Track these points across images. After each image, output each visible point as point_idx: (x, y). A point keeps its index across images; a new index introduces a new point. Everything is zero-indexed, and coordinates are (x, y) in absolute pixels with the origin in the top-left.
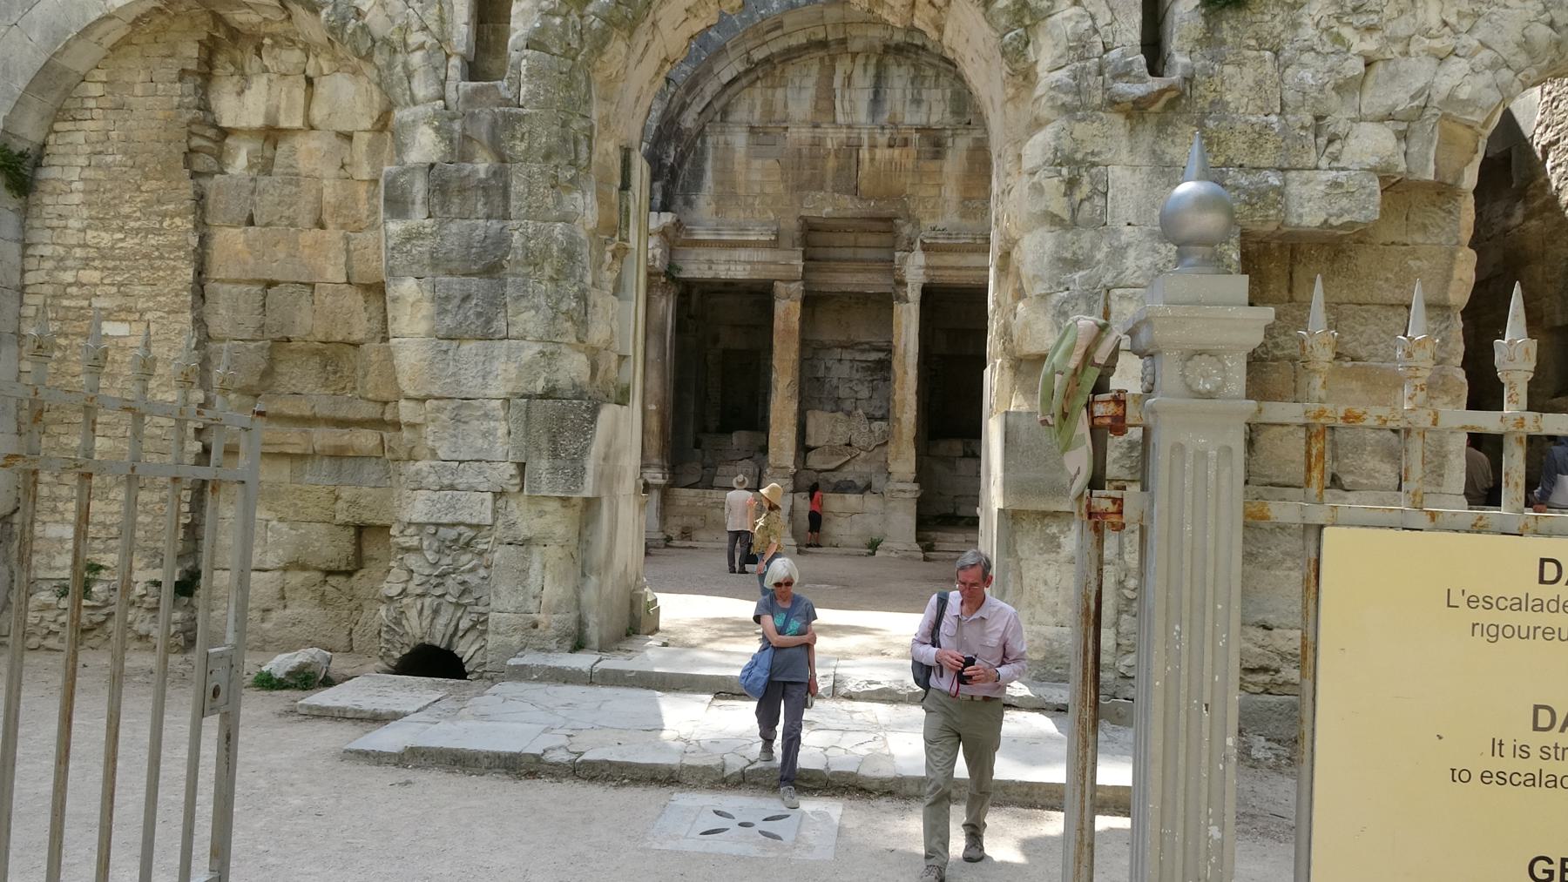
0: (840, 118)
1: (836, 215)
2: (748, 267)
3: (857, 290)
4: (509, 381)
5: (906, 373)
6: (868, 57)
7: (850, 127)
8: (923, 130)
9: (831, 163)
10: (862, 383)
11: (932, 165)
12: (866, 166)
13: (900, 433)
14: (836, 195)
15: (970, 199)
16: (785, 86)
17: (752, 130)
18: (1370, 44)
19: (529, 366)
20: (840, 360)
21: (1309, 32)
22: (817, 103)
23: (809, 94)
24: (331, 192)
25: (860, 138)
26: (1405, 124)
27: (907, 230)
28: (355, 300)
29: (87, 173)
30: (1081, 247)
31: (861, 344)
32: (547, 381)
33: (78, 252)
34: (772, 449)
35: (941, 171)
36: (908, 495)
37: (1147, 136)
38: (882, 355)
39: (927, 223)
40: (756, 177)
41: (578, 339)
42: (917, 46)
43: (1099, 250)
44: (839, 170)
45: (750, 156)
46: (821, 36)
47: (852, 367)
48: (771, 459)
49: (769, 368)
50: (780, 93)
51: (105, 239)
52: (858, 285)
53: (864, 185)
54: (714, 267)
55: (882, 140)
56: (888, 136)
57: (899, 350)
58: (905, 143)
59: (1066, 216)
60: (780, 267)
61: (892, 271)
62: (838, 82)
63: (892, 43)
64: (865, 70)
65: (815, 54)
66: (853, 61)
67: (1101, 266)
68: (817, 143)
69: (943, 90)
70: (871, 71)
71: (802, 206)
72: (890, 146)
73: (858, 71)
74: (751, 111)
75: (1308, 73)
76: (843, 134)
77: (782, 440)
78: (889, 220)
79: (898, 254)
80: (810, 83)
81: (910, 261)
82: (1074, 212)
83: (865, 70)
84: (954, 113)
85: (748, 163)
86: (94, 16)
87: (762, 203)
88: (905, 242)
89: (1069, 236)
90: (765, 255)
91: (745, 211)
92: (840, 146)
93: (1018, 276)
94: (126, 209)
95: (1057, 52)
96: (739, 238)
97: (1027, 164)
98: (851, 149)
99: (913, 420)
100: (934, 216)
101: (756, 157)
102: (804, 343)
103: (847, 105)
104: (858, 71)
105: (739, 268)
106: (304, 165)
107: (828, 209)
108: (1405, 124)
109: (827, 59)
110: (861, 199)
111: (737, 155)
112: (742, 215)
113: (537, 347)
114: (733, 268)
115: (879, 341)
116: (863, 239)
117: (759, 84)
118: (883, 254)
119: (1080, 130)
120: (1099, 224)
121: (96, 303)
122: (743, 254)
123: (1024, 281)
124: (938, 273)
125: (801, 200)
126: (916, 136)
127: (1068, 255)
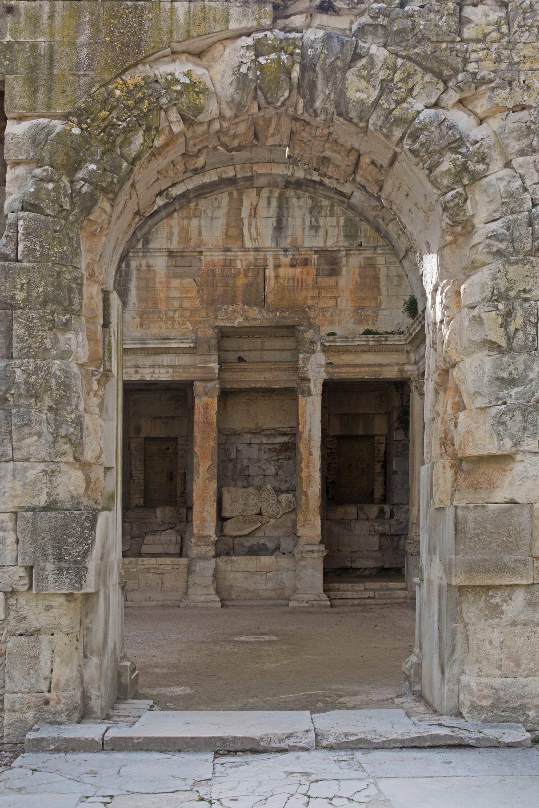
0: (248, 244)
1: (246, 324)
3: (264, 385)
4: (16, 496)
7: (257, 250)
9: (241, 281)
10: (270, 463)
12: (271, 283)
19: (34, 483)
20: (250, 444)
22: (227, 230)
23: (221, 223)
25: (265, 260)
30: (516, 369)
31: (268, 430)
32: (49, 494)
38: (286, 439)
41: (75, 458)
43: (532, 370)
44: (249, 286)
45: (172, 275)
46: (231, 174)
47: (260, 450)
49: (190, 452)
52: (265, 381)
53: (271, 298)
55: (285, 260)
56: (290, 257)
59: (503, 343)
61: (296, 369)
62: (245, 213)
63: (293, 180)
64: (269, 203)
65: (225, 189)
66: (258, 195)
67: (534, 383)
68: (228, 264)
69: (338, 218)
76: (251, 256)
78: (292, 327)
79: (301, 356)
80: (221, 213)
82: (510, 339)
83: (269, 203)
89: (505, 359)
92: (249, 265)
93: (457, 390)
95: (492, 207)
97: (466, 300)
102: (220, 431)
103: (253, 231)
104: (263, 203)
109: (235, 193)
110: (268, 310)
113: (41, 467)
115: (284, 427)
116: (269, 343)
118: (287, 356)
119: (513, 271)
123: (465, 396)
127: (505, 375)
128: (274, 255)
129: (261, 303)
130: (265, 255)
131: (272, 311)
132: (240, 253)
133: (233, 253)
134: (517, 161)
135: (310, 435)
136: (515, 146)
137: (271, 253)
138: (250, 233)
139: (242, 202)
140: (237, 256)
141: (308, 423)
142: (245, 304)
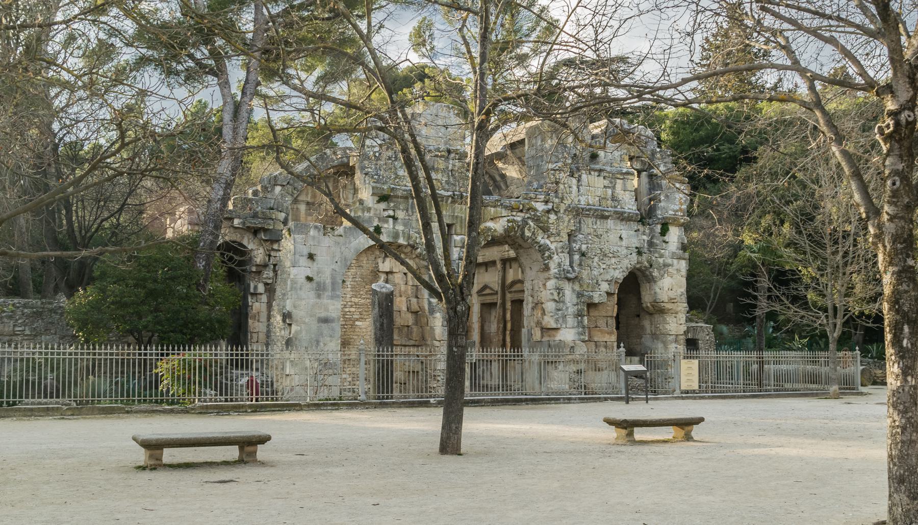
17: (308, 203)
18: (604, 266)
21: (595, 264)
24: (403, 288)
26: (609, 282)
28: (409, 315)
29: (352, 283)
33: (349, 303)
37: (571, 284)
51: (356, 300)
74: (307, 194)
75: (595, 272)
85: (306, 218)
86: (366, 247)
94: (362, 293)
106: (397, 281)
108: (609, 282)
120: (563, 302)
121: (354, 317)
134: (560, 254)
136: (560, 251)
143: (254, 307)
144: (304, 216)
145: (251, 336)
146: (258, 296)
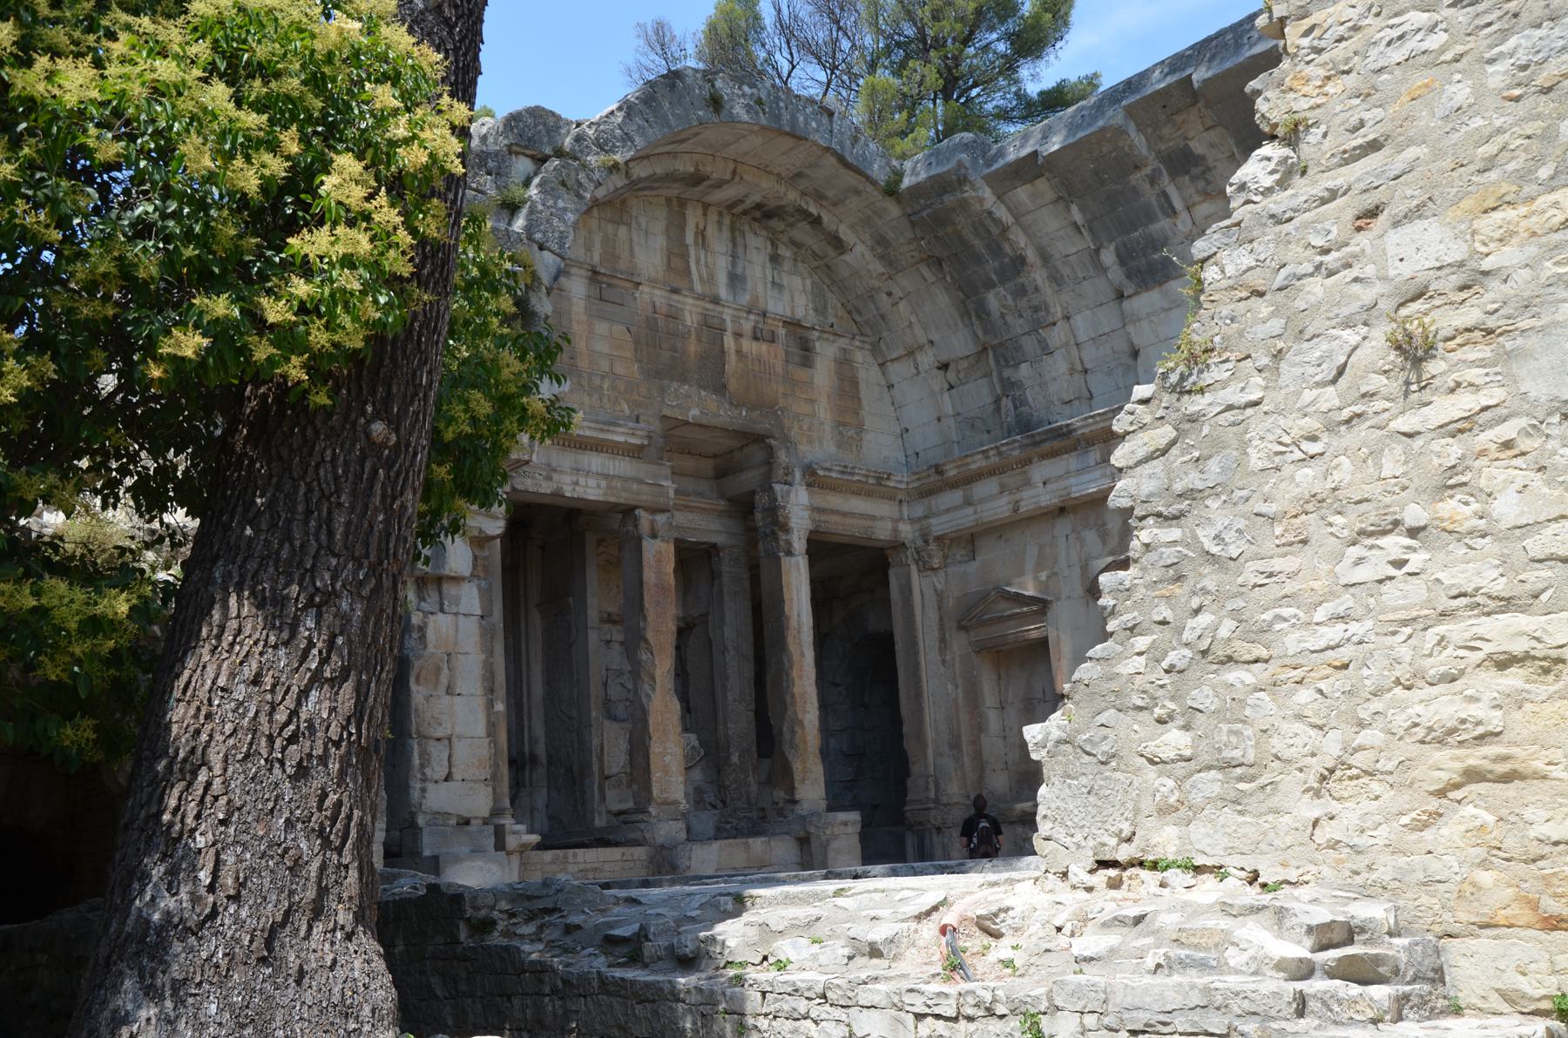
0: (698, 288)
1: (705, 422)
2: (603, 483)
5: (803, 655)
6: (720, 214)
8: (792, 324)
9: (693, 347)
11: (801, 374)
12: (732, 361)
13: (805, 742)
14: (703, 393)
15: (844, 425)
16: (629, 225)
23: (659, 242)
25: (724, 320)
27: (782, 456)
34: (656, 775)
35: (811, 384)
36: (850, 829)
39: (803, 448)
40: (602, 347)
42: (811, 215)
48: (655, 792)
50: (623, 231)
53: (733, 385)
54: (555, 476)
55: (747, 326)
57: (793, 623)
58: (772, 340)
60: (645, 488)
62: (690, 238)
68: (674, 316)
70: (726, 234)
71: (663, 401)
72: (756, 338)
73: (711, 230)
74: (589, 248)
77: (667, 758)
81: (792, 495)
84: (816, 310)
87: (613, 387)
88: (781, 472)
90: (621, 466)
91: (590, 395)
96: (602, 436)
98: (712, 328)
99: (816, 722)
100: (811, 442)
101: (602, 318)
105: (592, 482)
107: (694, 413)
110: (731, 403)
111: (574, 308)
112: (586, 400)
114: (582, 481)
117: (595, 212)
122: (595, 461)
124: (824, 518)
125: (662, 390)
126: (781, 331)
128: (733, 316)
129: (720, 389)
130: (722, 313)
131: (737, 406)
132: (690, 301)
133: (680, 298)
135: (799, 621)
137: (730, 311)
138: (699, 271)
139: (685, 219)
140: (685, 303)
141: (795, 602)
142: (701, 387)
143: (430, 635)
144: (584, 318)
145: (424, 754)
146: (449, 589)
